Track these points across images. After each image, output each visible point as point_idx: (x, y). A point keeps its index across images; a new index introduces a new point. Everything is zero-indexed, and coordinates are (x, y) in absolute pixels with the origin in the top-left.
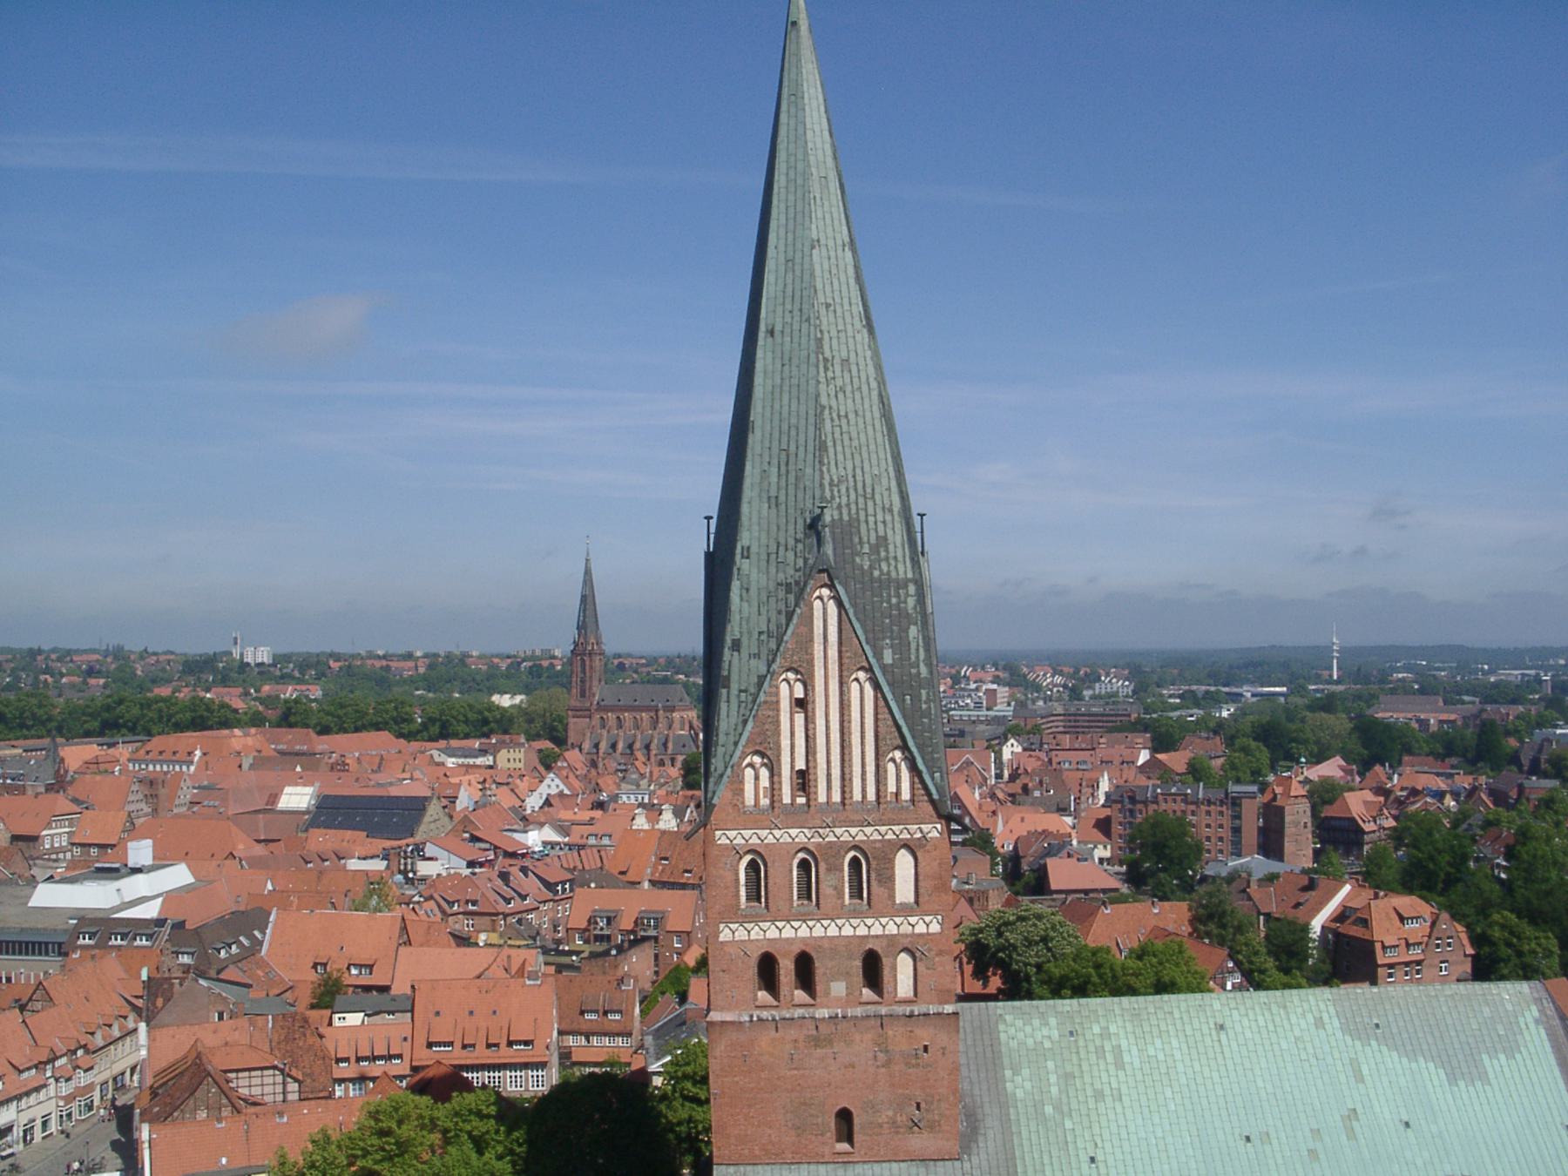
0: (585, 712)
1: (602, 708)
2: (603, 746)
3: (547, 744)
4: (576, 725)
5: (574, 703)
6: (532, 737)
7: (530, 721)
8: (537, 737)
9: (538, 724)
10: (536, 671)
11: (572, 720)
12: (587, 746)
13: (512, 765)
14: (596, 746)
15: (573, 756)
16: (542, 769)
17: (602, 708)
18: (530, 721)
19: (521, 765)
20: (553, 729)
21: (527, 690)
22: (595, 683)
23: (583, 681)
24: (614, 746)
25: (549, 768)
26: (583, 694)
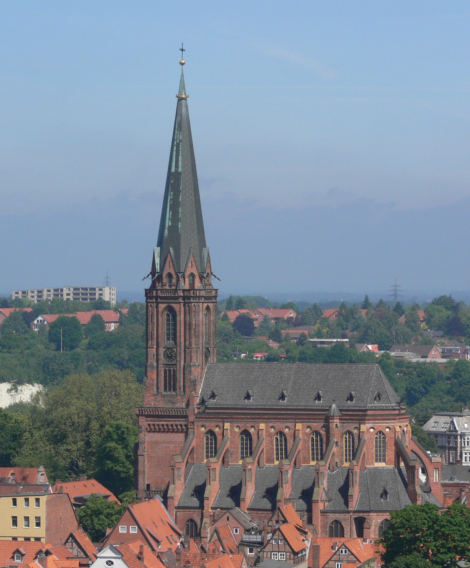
0: (172, 421)
1: (208, 412)
2: (214, 492)
3: (91, 488)
4: (155, 448)
5: (152, 401)
6: (61, 472)
7: (59, 439)
8: (73, 471)
9: (74, 446)
10: (64, 334)
11: (147, 438)
12: (178, 492)
13: (21, 531)
14: (199, 492)
15: (151, 513)
16: (84, 539)
17: (208, 412)
18: (59, 439)
19: (41, 532)
20: (108, 455)
21: (45, 374)
22: (197, 359)
23: (171, 355)
24: (235, 493)
25: (99, 538)
26: (171, 382)
